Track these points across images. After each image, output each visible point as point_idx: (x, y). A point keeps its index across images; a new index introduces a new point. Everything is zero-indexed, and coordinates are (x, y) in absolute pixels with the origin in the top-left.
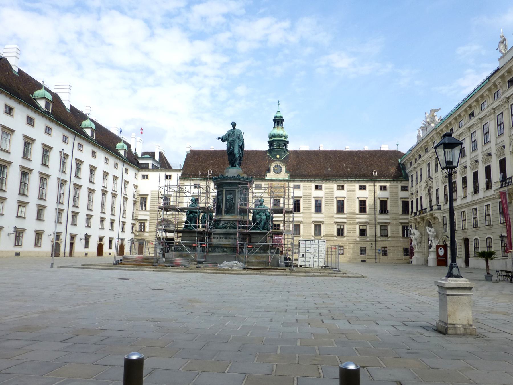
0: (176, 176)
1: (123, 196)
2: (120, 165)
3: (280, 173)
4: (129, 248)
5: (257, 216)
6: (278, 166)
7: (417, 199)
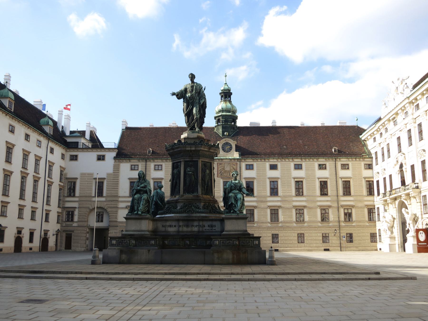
0: (110, 156)
1: (47, 180)
2: (44, 141)
3: (229, 151)
4: (54, 242)
5: (231, 194)
6: (227, 144)
7: (385, 179)
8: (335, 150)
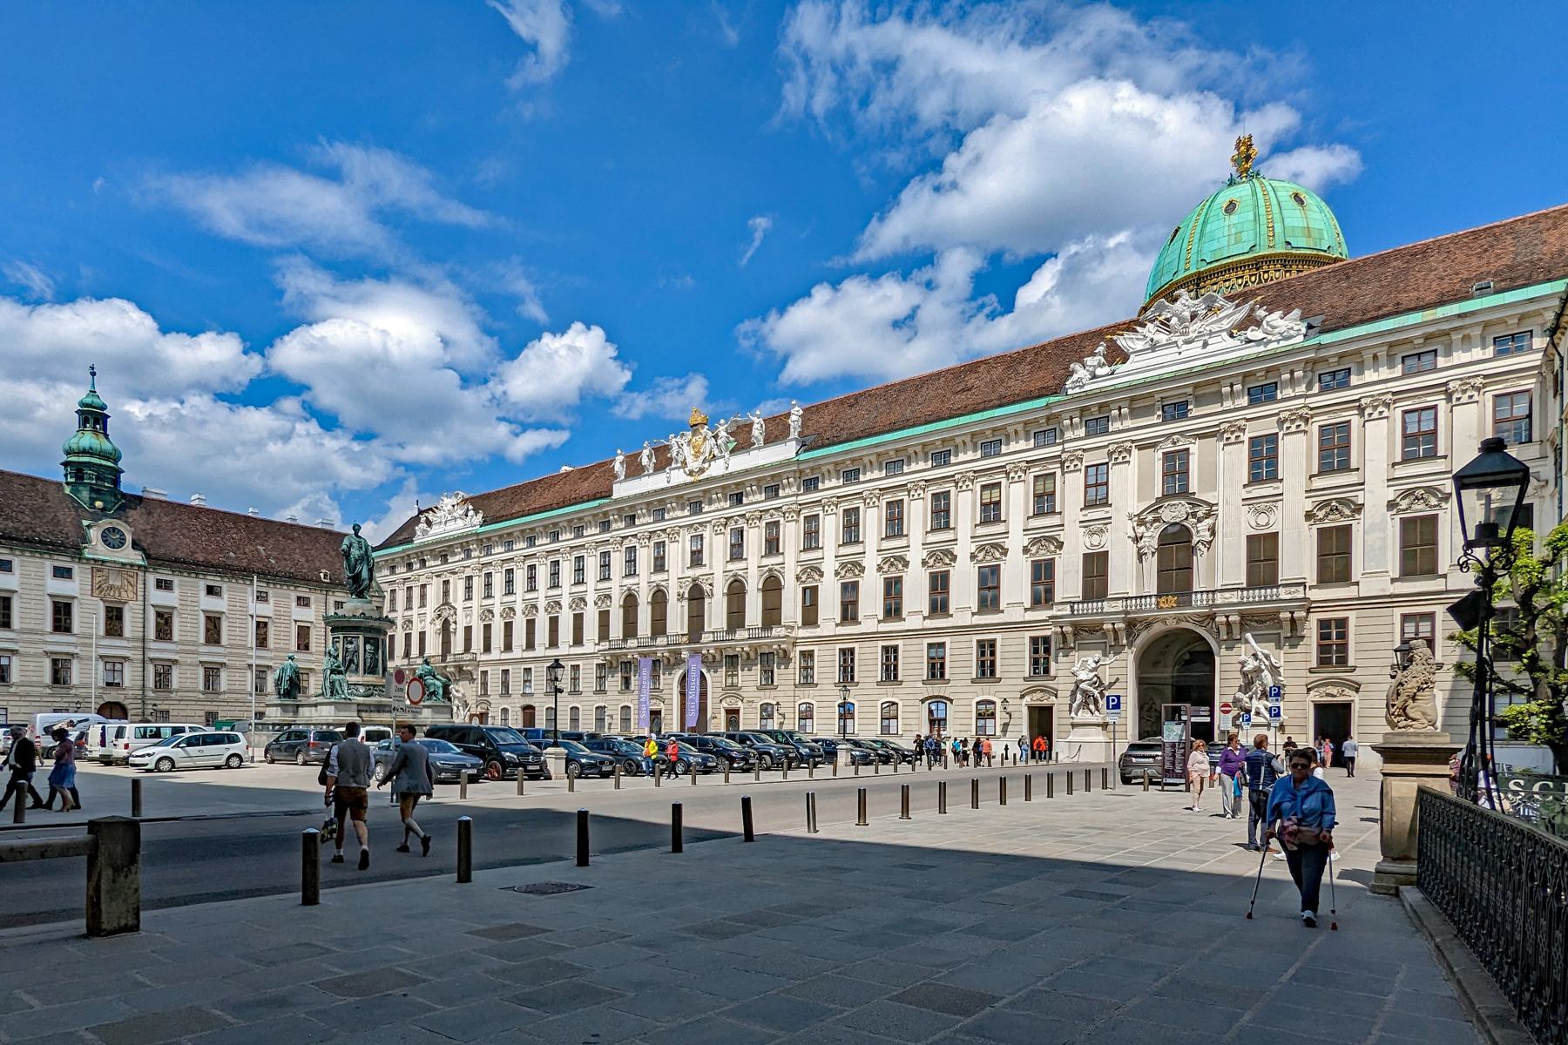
7: (408, 636)
8: (325, 575)
